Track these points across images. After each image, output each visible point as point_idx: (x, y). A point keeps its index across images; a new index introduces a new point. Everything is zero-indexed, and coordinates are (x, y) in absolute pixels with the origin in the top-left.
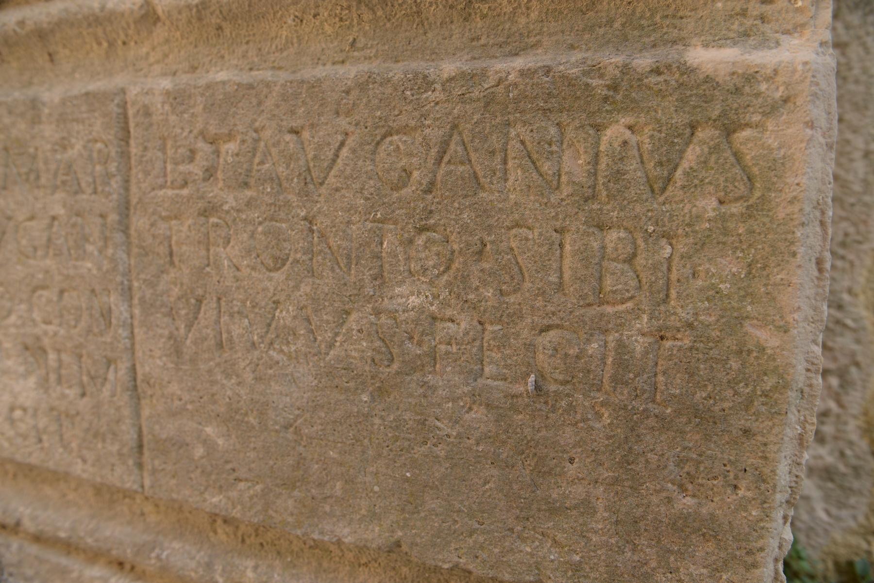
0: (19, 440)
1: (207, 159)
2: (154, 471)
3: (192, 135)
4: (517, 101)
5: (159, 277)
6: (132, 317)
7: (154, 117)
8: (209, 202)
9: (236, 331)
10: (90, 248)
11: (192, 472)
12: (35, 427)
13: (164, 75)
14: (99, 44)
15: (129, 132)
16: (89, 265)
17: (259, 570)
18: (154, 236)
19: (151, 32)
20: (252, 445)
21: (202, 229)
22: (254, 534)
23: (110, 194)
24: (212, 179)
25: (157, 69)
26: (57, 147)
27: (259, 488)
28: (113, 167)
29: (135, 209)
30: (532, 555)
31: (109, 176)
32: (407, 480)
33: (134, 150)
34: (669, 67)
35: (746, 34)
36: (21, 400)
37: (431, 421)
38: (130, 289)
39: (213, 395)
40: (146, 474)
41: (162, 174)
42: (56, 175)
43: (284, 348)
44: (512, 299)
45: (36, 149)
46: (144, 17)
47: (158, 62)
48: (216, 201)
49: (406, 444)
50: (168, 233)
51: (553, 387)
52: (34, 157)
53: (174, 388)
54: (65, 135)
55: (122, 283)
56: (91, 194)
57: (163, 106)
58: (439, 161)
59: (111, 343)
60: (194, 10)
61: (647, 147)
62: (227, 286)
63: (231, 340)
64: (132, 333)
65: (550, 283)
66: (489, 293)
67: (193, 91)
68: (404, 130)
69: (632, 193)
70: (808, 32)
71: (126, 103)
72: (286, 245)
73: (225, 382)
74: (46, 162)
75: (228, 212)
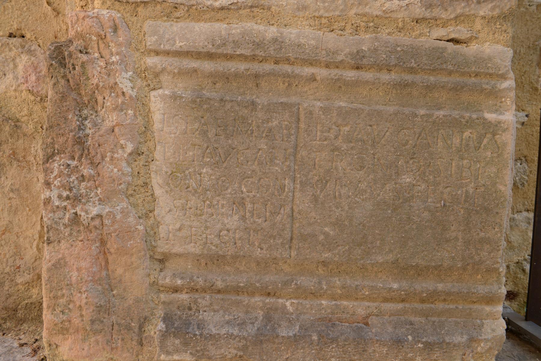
0: (223, 245)
4: (442, 123)
6: (294, 188)
9: (343, 191)
14: (283, 84)
16: (277, 168)
18: (309, 158)
23: (290, 141)
25: (312, 97)
27: (347, 248)
28: (293, 132)
29: (301, 147)
30: (440, 256)
32: (403, 237)
33: (302, 125)
34: (481, 118)
35: (497, 111)
36: (228, 226)
37: (412, 217)
38: (294, 178)
42: (263, 132)
43: (361, 197)
44: (437, 179)
45: (252, 121)
46: (310, 79)
47: (311, 95)
49: (403, 225)
51: (448, 204)
52: (251, 124)
58: (418, 138)
61: (475, 138)
63: (340, 195)
65: (448, 174)
66: (431, 177)
68: (408, 128)
69: (471, 150)
70: (510, 111)
72: (365, 162)
74: (258, 127)
75: (343, 151)
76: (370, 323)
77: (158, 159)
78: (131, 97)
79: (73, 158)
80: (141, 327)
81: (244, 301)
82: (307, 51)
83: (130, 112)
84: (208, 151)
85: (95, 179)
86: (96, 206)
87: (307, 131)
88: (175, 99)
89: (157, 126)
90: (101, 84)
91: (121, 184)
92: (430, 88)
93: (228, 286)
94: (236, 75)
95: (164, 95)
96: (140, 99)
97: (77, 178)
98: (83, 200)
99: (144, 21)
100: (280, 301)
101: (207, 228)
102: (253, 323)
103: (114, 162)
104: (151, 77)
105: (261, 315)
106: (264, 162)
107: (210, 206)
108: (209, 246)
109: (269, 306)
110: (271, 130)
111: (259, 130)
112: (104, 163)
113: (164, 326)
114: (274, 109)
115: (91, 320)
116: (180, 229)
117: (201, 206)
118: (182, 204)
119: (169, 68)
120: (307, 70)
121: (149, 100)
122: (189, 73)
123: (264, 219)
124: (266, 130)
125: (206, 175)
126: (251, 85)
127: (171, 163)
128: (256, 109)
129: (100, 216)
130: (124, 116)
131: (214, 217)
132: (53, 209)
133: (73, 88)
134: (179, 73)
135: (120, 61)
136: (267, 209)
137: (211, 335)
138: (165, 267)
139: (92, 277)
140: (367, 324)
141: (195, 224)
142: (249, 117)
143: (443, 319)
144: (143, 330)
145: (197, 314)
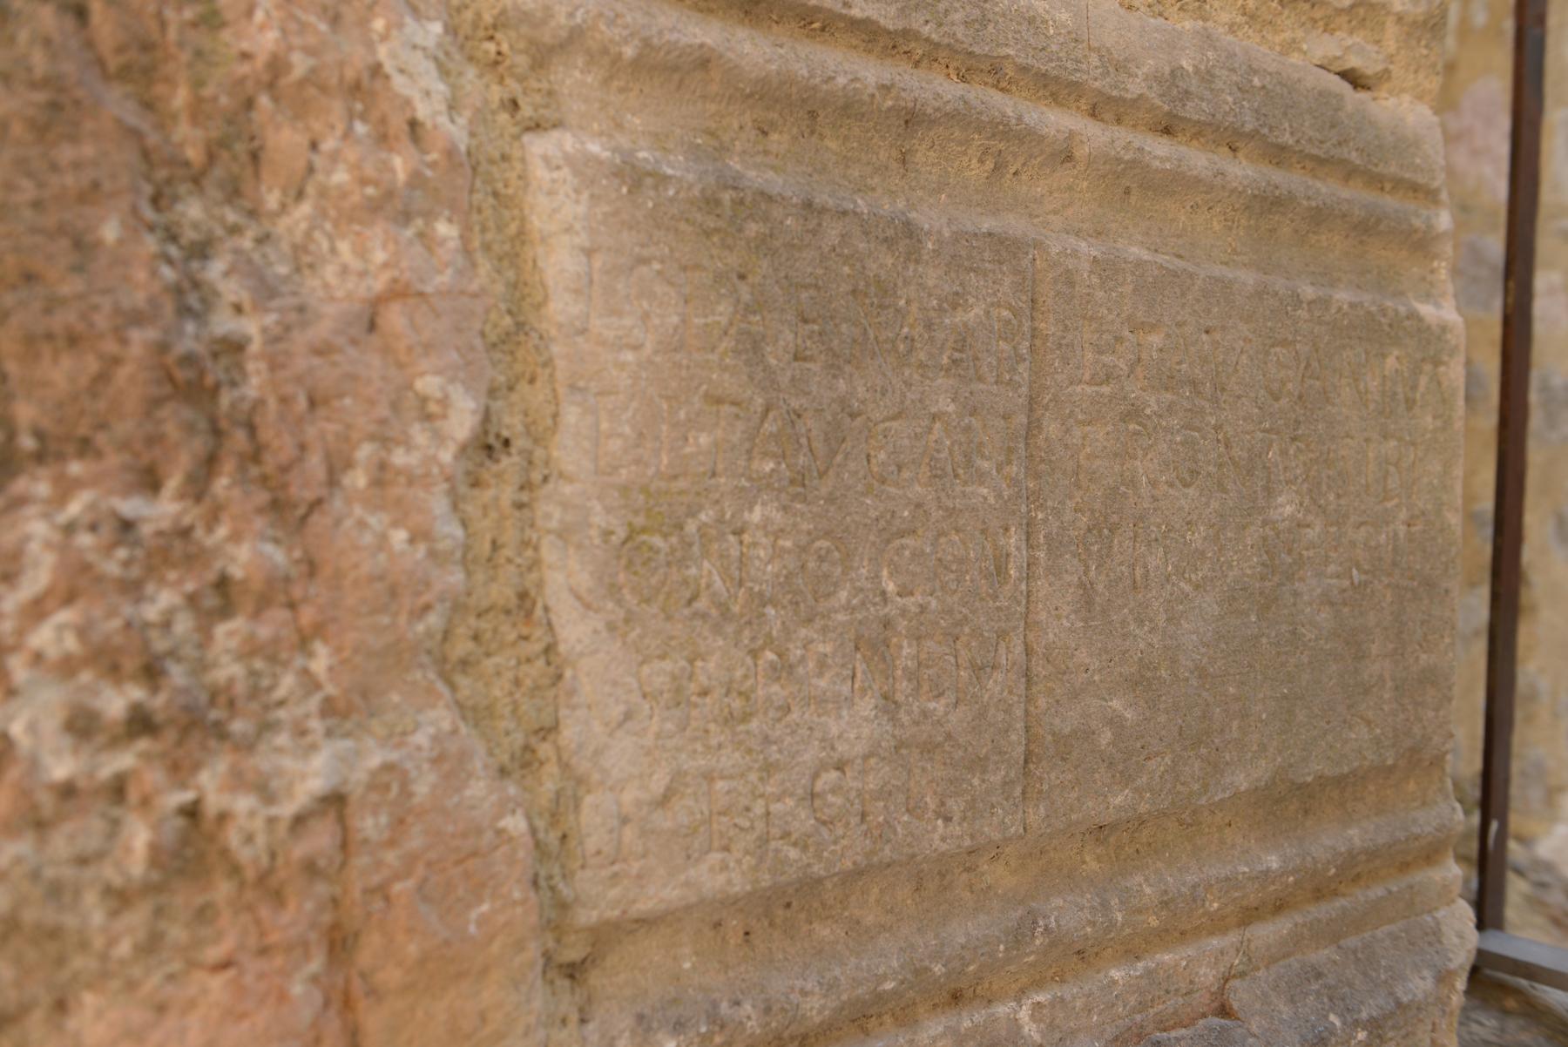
0: (824, 831)
14: (981, 161)
20: (1162, 706)
27: (1168, 760)
32: (1285, 697)
36: (841, 748)
45: (908, 302)
53: (1082, 656)
54: (959, 289)
66: (1332, 497)
75: (1149, 417)
76: (1235, 1005)
77: (570, 468)
79: (150, 482)
83: (443, 229)
84: (769, 427)
85: (297, 592)
86: (313, 748)
89: (561, 307)
90: (300, 64)
91: (427, 608)
92: (1319, 217)
94: (846, 107)
97: (192, 600)
101: (769, 769)
103: (397, 491)
104: (522, 61)
106: (949, 469)
108: (777, 851)
111: (931, 339)
114: (970, 258)
116: (664, 801)
117: (746, 677)
118: (674, 678)
119: (606, 32)
122: (676, 69)
125: (760, 534)
126: (883, 155)
127: (625, 490)
129: (335, 802)
131: (794, 716)
132: (35, 807)
133: (113, 63)
134: (636, 63)
140: (1224, 1011)
141: (730, 759)
142: (900, 284)
143: (1367, 935)
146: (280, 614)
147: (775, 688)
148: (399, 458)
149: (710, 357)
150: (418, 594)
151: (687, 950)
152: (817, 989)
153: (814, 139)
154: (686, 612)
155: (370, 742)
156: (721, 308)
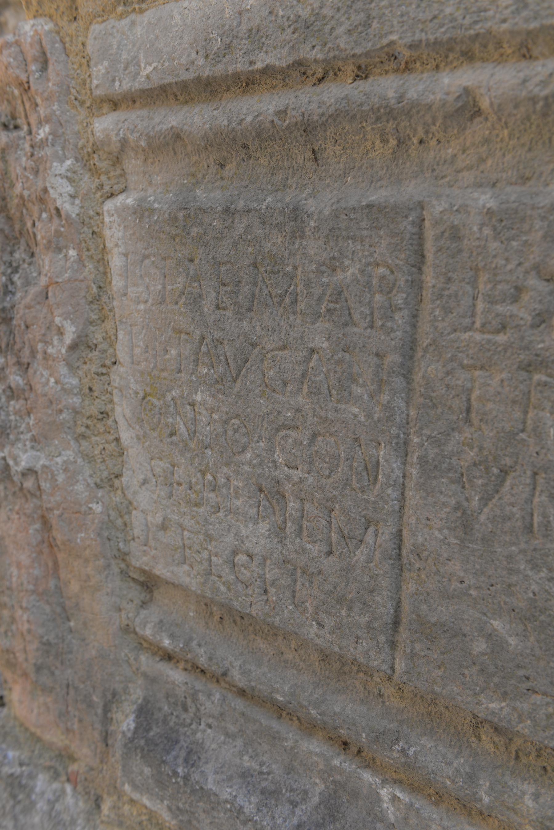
0: (240, 587)
1: (540, 301)
2: (413, 656)
3: (521, 269)
5: (449, 435)
6: (404, 477)
7: (466, 242)
8: (537, 355)
10: (358, 390)
11: (467, 667)
12: (262, 577)
13: (479, 185)
14: (385, 141)
15: (423, 256)
16: (357, 410)
17: (542, 800)
18: (448, 386)
19: (464, 129)
21: (522, 387)
22: (534, 754)
23: (392, 330)
24: (543, 326)
25: (468, 177)
26: (324, 268)
28: (399, 299)
29: (425, 350)
31: (392, 308)
33: (429, 278)
36: (248, 545)
39: (510, 586)
40: (398, 656)
41: (469, 314)
42: (320, 300)
45: (295, 268)
46: (459, 111)
47: (469, 168)
48: (548, 354)
50: (469, 385)
53: (455, 567)
55: (398, 436)
56: (366, 328)
57: (480, 229)
59: (374, 503)
60: (541, 104)
62: (550, 461)
64: (403, 494)
67: (529, 212)
71: (424, 220)
73: (530, 573)
74: (308, 284)
77: (121, 360)
78: (68, 217)
80: (106, 710)
81: (286, 739)
82: (448, 10)
84: (204, 349)
85: (27, 395)
87: (440, 296)
88: (141, 218)
89: (117, 283)
90: (26, 193)
91: (61, 411)
93: (253, 689)
94: (259, 135)
95: (125, 208)
96: (87, 220)
98: (11, 437)
99: (88, 29)
100: (367, 776)
102: (294, 804)
103: (50, 362)
104: (103, 165)
105: (318, 790)
106: (324, 389)
107: (214, 488)
109: (338, 778)
110: (340, 293)
111: (310, 295)
112: (36, 365)
113: (133, 726)
115: (35, 665)
116: (164, 527)
117: (197, 483)
120: (446, 81)
121: (102, 223)
122: (168, 144)
123: (325, 549)
124: (329, 292)
127: (142, 373)
128: (303, 232)
129: (30, 472)
130: (62, 263)
131: (221, 514)
135: (50, 137)
136: (333, 520)
137: (202, 788)
138: (151, 600)
139: (34, 585)
144: (109, 715)
145: (194, 726)
146: (22, 402)
147: (212, 495)
148: (50, 350)
149: (174, 307)
150: (58, 405)
151: (193, 607)
152: (237, 668)
153: (251, 161)
154: (169, 440)
155: (43, 456)
156: (179, 280)
